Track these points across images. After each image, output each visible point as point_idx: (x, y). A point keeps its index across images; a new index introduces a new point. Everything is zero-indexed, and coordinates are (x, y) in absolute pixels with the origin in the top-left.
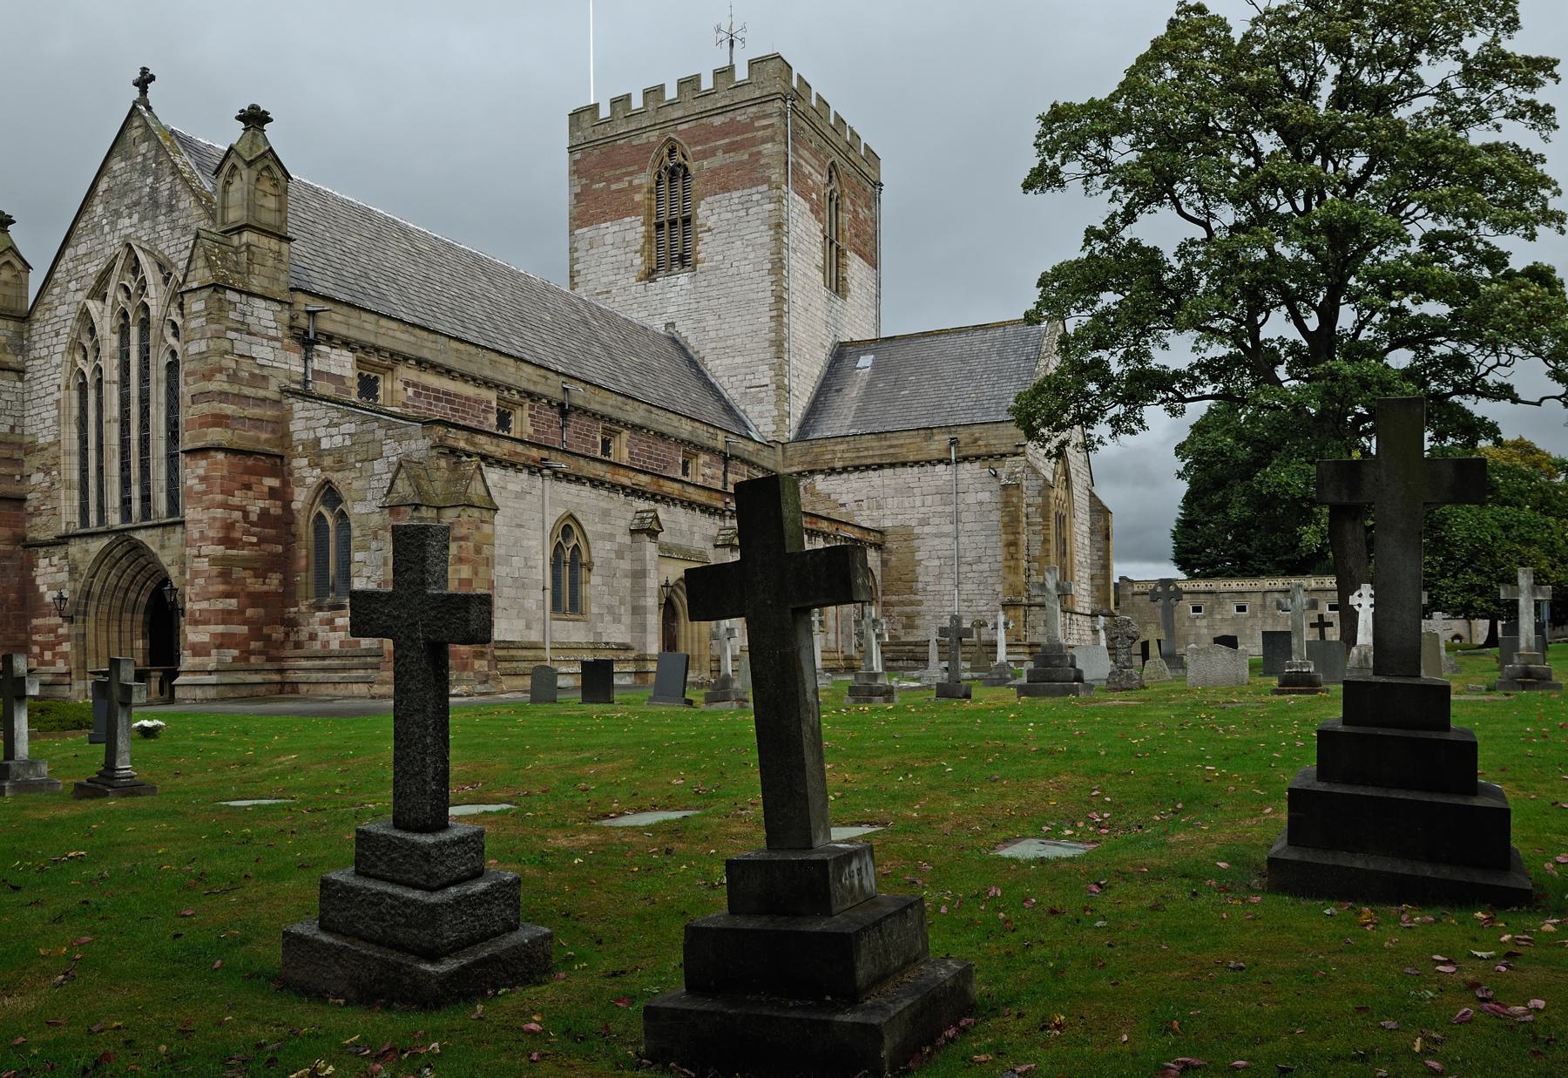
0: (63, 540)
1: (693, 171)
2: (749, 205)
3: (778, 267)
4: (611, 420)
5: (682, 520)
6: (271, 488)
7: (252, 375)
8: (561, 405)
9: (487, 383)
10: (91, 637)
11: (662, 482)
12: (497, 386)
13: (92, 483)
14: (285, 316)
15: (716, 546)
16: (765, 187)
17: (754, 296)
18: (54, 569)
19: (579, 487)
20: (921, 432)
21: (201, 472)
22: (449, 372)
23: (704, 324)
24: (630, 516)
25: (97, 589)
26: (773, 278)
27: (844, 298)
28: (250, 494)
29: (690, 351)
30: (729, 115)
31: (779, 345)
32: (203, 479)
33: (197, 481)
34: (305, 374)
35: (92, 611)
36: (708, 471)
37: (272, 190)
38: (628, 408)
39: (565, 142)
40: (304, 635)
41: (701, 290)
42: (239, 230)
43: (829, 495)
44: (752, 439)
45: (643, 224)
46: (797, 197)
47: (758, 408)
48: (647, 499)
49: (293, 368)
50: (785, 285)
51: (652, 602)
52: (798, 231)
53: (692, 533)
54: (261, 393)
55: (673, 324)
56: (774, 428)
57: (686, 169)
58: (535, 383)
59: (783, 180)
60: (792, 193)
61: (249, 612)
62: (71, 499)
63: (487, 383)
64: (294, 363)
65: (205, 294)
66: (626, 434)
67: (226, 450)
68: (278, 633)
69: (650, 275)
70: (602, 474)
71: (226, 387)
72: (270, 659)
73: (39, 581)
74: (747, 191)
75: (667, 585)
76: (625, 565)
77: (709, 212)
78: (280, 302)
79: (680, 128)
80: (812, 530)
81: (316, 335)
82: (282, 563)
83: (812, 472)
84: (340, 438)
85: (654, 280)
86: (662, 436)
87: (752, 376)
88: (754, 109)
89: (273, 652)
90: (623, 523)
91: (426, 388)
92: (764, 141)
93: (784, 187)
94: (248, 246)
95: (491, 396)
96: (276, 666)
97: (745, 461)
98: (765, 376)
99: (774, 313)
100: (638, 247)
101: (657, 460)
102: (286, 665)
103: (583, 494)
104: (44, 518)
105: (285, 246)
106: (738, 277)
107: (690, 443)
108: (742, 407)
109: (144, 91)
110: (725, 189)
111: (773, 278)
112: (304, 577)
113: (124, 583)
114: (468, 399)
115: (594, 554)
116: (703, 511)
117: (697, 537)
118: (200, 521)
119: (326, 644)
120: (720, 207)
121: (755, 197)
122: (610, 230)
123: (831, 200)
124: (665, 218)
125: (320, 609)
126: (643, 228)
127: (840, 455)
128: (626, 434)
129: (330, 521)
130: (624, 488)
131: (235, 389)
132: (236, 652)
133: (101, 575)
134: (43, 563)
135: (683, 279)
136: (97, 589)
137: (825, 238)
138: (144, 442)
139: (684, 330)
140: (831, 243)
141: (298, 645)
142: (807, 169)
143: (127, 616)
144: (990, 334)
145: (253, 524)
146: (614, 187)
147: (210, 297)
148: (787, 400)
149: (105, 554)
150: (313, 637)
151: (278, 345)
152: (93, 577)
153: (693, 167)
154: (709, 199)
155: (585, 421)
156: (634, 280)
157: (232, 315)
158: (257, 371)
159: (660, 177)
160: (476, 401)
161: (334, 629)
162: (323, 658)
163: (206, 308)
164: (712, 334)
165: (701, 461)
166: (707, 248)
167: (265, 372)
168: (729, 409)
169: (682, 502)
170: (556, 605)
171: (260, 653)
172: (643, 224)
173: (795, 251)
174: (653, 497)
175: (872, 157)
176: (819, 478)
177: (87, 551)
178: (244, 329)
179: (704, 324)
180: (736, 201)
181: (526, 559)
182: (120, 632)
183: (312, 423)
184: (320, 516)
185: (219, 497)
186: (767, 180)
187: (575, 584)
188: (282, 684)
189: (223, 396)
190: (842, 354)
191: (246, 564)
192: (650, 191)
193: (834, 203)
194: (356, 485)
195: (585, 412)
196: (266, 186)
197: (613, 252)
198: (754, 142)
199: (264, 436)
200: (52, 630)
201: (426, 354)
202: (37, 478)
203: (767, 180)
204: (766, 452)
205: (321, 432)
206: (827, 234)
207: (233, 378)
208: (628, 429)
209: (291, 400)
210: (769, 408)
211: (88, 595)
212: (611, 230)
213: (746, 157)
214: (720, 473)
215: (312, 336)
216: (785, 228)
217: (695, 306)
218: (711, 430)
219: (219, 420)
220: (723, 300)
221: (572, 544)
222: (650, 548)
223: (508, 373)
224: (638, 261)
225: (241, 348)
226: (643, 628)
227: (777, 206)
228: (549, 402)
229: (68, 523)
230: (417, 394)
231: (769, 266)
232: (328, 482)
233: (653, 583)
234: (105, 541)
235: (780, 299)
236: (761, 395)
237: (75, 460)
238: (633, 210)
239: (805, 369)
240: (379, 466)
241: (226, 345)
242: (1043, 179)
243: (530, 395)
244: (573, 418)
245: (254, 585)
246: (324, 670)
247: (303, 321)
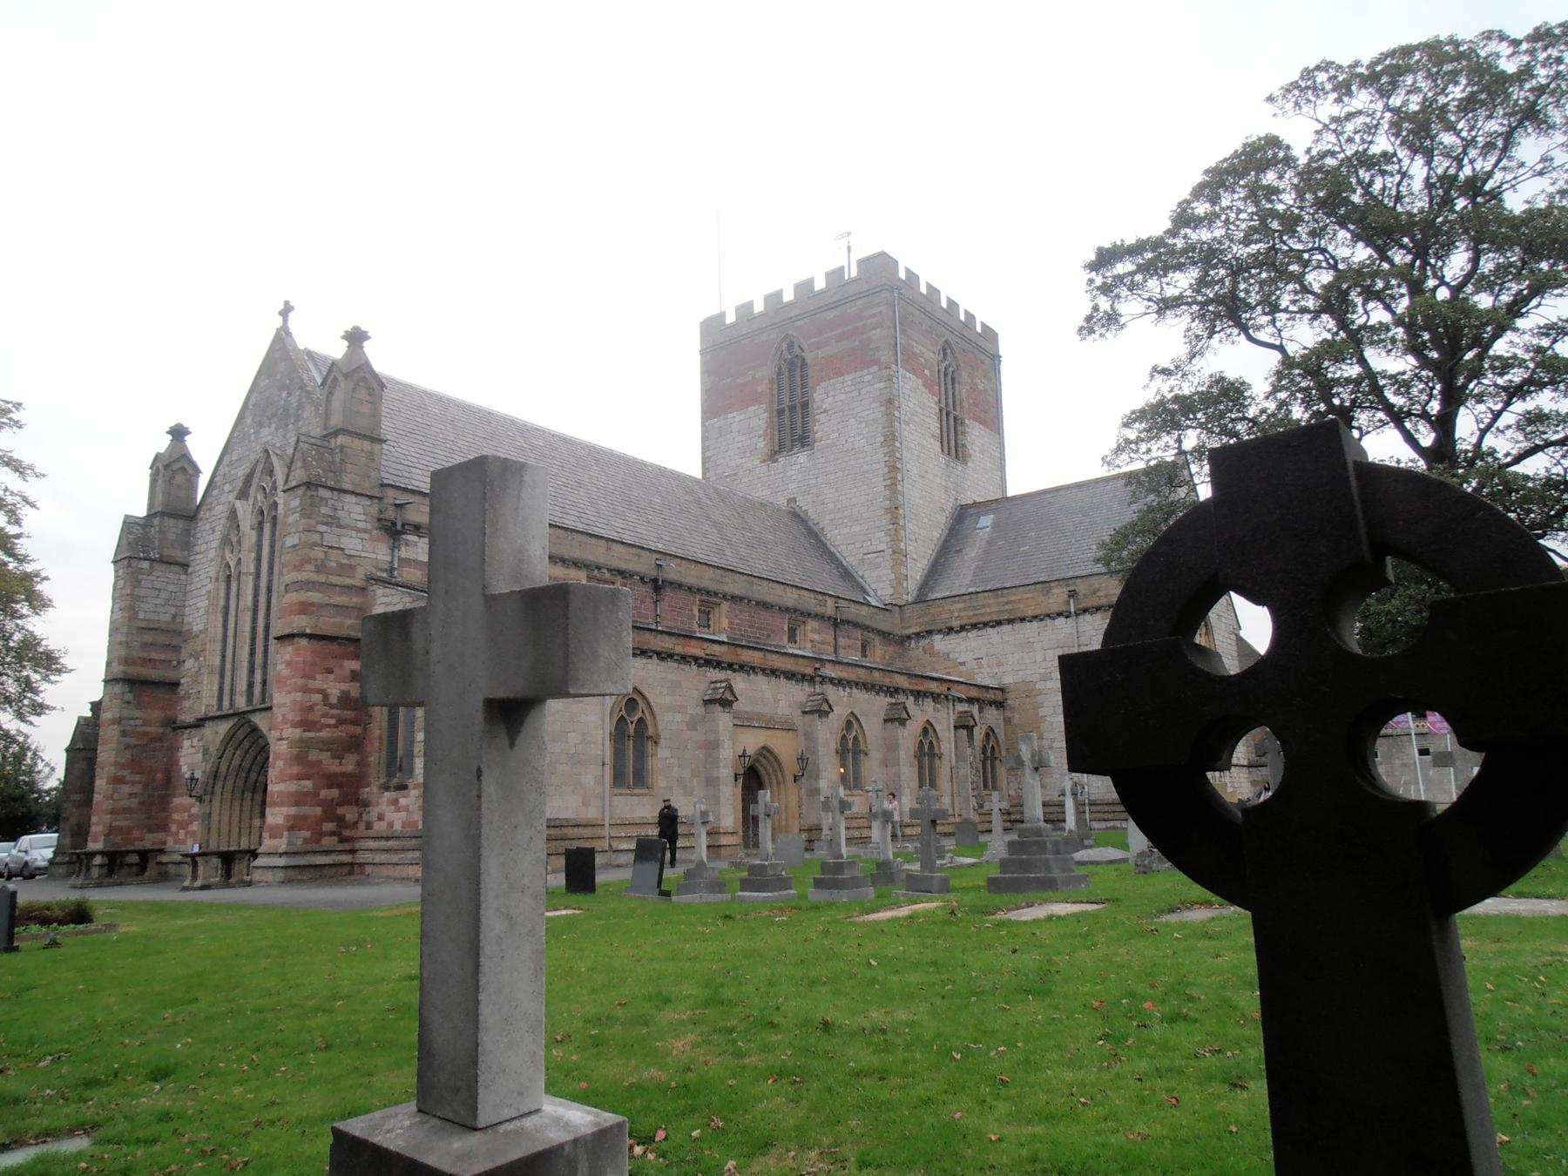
0: (200, 723)
1: (809, 361)
2: (861, 386)
3: (891, 439)
4: (708, 593)
6: (352, 672)
7: (341, 565)
8: (655, 581)
9: (576, 564)
10: (215, 817)
11: (739, 650)
12: (587, 566)
13: (228, 666)
14: (375, 509)
15: (805, 713)
16: (876, 368)
17: (866, 468)
18: (193, 750)
19: (645, 661)
20: (1037, 586)
21: (287, 657)
23: (823, 497)
24: (703, 686)
25: (223, 769)
26: (886, 450)
27: (965, 462)
28: (331, 677)
29: (811, 524)
30: (840, 309)
31: (894, 511)
33: (283, 666)
34: (392, 562)
35: (218, 790)
36: (816, 637)
37: (368, 398)
38: (727, 580)
39: (699, 349)
40: (373, 813)
41: (819, 466)
42: (335, 434)
43: (948, 654)
44: (869, 605)
45: (766, 412)
46: (907, 374)
47: (875, 573)
48: (723, 668)
49: (380, 557)
50: (898, 455)
51: (726, 772)
52: (911, 405)
53: (776, 701)
54: (348, 581)
55: (794, 500)
56: (891, 591)
57: (803, 360)
59: (893, 359)
60: (902, 371)
61: (324, 793)
62: (211, 683)
63: (576, 564)
64: (380, 553)
65: (300, 491)
66: (725, 605)
67: (310, 637)
68: (350, 813)
69: (773, 456)
70: (671, 646)
71: (313, 576)
72: (342, 840)
73: (182, 762)
74: (858, 374)
75: (743, 756)
76: (697, 736)
77: (823, 396)
78: (370, 497)
79: (796, 324)
80: (919, 692)
81: (403, 525)
82: (355, 745)
83: (930, 632)
85: (776, 461)
86: (765, 605)
87: (869, 543)
88: (861, 302)
89: (346, 833)
90: (695, 694)
92: (875, 328)
93: (894, 366)
94: (342, 447)
96: (347, 846)
97: (856, 625)
98: (881, 541)
99: (888, 482)
100: (761, 432)
101: (760, 628)
102: (357, 845)
103: (649, 667)
104: (191, 701)
105: (377, 446)
106: (853, 452)
107: (795, 610)
108: (860, 573)
109: (285, 320)
110: (839, 374)
111: (886, 450)
112: (375, 756)
113: (246, 764)
115: (661, 726)
116: (787, 678)
117: (782, 704)
119: (391, 825)
120: (834, 390)
121: (866, 379)
122: (736, 419)
123: (946, 375)
124: (786, 403)
126: (766, 415)
127: (958, 613)
130: (696, 659)
131: (322, 578)
132: (307, 834)
133: (228, 753)
134: (186, 743)
135: (802, 457)
136: (223, 769)
137: (941, 410)
139: (805, 504)
140: (948, 415)
141: (369, 826)
142: (918, 349)
143: (248, 795)
145: (332, 707)
146: (739, 381)
147: (304, 494)
148: (904, 564)
149: (231, 736)
150: (381, 817)
151: (366, 536)
152: (220, 758)
153: (809, 357)
154: (824, 384)
155: (681, 594)
156: (758, 461)
157: (324, 510)
158: (345, 561)
159: (780, 368)
161: (398, 810)
162: (388, 838)
163: (301, 505)
164: (831, 506)
165: (809, 627)
166: (823, 428)
167: (353, 562)
168: (847, 575)
169: (763, 670)
170: (619, 778)
171: (332, 833)
172: (766, 412)
173: (908, 423)
174: (730, 666)
175: (990, 335)
176: (937, 638)
177: (217, 733)
178: (333, 521)
179: (823, 497)
180: (849, 383)
181: (583, 735)
182: (241, 810)
185: (300, 681)
186: (877, 362)
187: (641, 757)
188: (352, 864)
189: (308, 585)
190: (962, 516)
191: (324, 745)
192: (771, 382)
193: (949, 378)
195: (680, 586)
196: (363, 395)
197: (740, 438)
199: (350, 622)
200: (187, 809)
202: (190, 663)
203: (877, 362)
204: (882, 616)
206: (943, 406)
207: (320, 568)
208: (726, 600)
209: (375, 587)
210: (886, 572)
211: (216, 775)
212: (737, 419)
213: (857, 343)
214: (830, 638)
215: (399, 527)
216: (896, 404)
217: (814, 481)
218: (819, 597)
219: (304, 608)
220: (840, 474)
221: (636, 718)
222: (723, 719)
223: (597, 554)
224: (761, 444)
225: (330, 540)
226: (717, 801)
227: (887, 384)
228: (642, 579)
229: (207, 706)
231: (882, 439)
233: (727, 753)
235: (893, 469)
236: (878, 560)
238: (755, 400)
239: (923, 532)
241: (316, 537)
242: (1100, 322)
243: (621, 573)
244: (668, 593)
245: (333, 766)
246: (387, 851)
247: (391, 514)
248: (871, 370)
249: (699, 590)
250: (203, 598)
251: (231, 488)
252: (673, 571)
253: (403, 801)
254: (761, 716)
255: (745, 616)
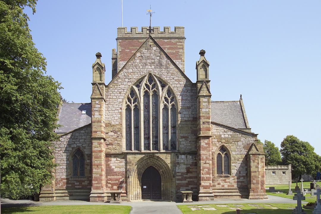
16: (180, 61)
32: (206, 144)
33: (205, 144)
84: (228, 136)
92: (180, 49)
118: (206, 154)
125: (221, 177)
129: (223, 156)
138: (137, 128)
144: (225, 104)
183: (218, 131)
184: (219, 154)
194: (232, 147)
198: (177, 48)
205: (221, 133)
232: (223, 146)
234: (144, 156)
240: (240, 143)
248: (179, 61)
250: (116, 114)
251: (129, 81)
253: (227, 180)
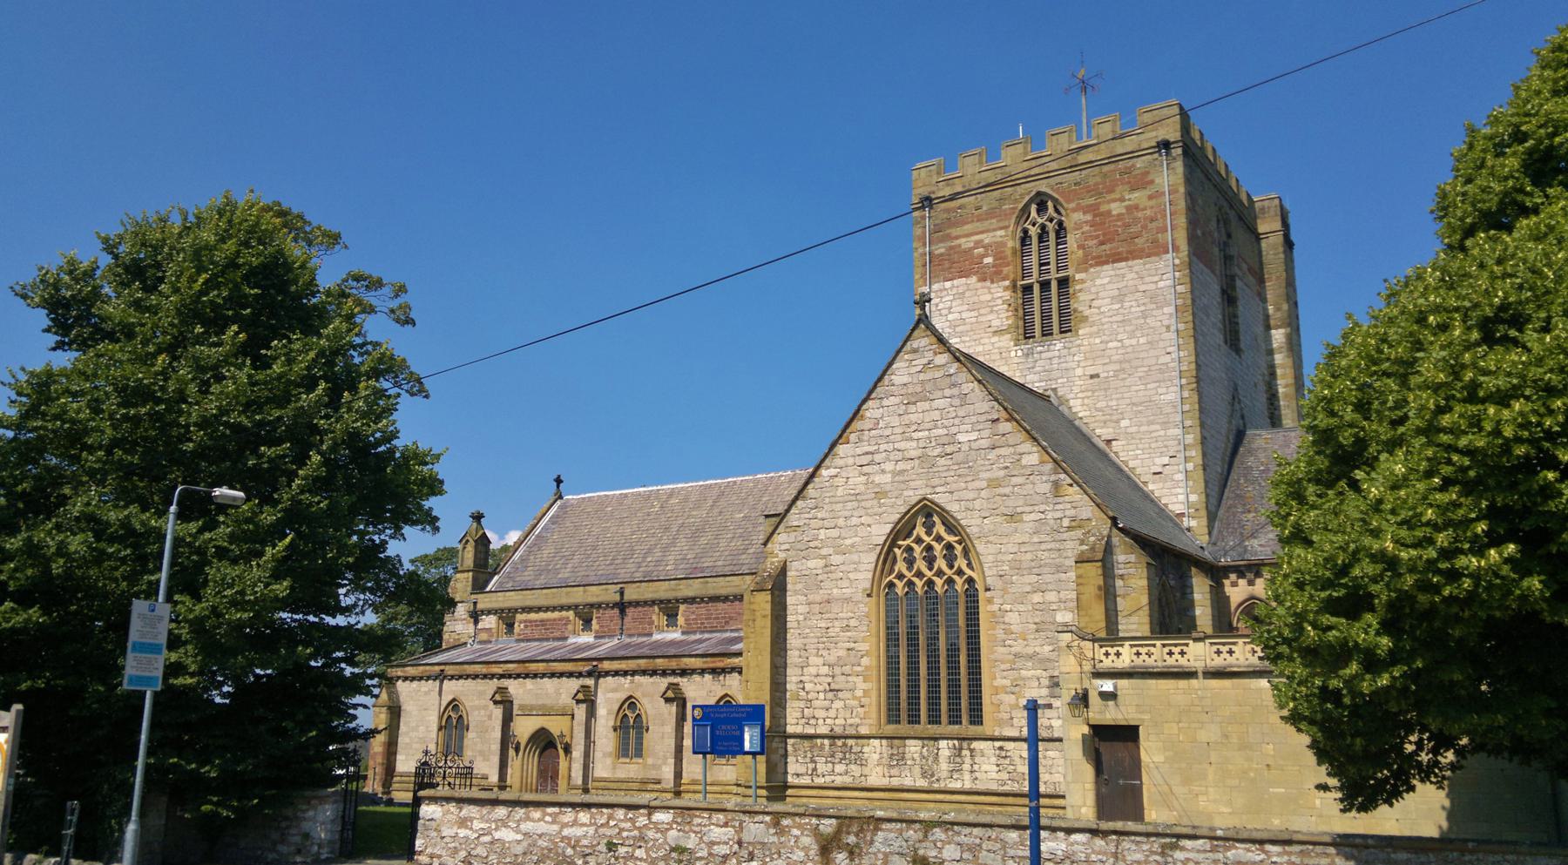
4: (661, 602)
5: (548, 686)
9: (562, 608)
11: (527, 665)
22: (539, 609)
58: (597, 596)
63: (562, 608)
66: (682, 607)
91: (531, 621)
95: (571, 614)
101: (718, 618)
114: (555, 620)
117: (563, 696)
128: (682, 607)
160: (560, 620)
201: (528, 603)
208: (682, 603)
230: (526, 627)
237: (630, 661)
243: (592, 605)
244: (630, 612)
249: (653, 602)
252: (631, 594)
254: (543, 707)
255: (703, 611)
